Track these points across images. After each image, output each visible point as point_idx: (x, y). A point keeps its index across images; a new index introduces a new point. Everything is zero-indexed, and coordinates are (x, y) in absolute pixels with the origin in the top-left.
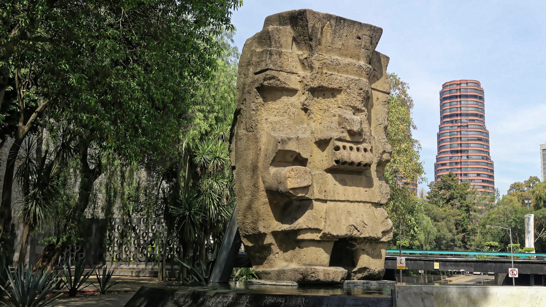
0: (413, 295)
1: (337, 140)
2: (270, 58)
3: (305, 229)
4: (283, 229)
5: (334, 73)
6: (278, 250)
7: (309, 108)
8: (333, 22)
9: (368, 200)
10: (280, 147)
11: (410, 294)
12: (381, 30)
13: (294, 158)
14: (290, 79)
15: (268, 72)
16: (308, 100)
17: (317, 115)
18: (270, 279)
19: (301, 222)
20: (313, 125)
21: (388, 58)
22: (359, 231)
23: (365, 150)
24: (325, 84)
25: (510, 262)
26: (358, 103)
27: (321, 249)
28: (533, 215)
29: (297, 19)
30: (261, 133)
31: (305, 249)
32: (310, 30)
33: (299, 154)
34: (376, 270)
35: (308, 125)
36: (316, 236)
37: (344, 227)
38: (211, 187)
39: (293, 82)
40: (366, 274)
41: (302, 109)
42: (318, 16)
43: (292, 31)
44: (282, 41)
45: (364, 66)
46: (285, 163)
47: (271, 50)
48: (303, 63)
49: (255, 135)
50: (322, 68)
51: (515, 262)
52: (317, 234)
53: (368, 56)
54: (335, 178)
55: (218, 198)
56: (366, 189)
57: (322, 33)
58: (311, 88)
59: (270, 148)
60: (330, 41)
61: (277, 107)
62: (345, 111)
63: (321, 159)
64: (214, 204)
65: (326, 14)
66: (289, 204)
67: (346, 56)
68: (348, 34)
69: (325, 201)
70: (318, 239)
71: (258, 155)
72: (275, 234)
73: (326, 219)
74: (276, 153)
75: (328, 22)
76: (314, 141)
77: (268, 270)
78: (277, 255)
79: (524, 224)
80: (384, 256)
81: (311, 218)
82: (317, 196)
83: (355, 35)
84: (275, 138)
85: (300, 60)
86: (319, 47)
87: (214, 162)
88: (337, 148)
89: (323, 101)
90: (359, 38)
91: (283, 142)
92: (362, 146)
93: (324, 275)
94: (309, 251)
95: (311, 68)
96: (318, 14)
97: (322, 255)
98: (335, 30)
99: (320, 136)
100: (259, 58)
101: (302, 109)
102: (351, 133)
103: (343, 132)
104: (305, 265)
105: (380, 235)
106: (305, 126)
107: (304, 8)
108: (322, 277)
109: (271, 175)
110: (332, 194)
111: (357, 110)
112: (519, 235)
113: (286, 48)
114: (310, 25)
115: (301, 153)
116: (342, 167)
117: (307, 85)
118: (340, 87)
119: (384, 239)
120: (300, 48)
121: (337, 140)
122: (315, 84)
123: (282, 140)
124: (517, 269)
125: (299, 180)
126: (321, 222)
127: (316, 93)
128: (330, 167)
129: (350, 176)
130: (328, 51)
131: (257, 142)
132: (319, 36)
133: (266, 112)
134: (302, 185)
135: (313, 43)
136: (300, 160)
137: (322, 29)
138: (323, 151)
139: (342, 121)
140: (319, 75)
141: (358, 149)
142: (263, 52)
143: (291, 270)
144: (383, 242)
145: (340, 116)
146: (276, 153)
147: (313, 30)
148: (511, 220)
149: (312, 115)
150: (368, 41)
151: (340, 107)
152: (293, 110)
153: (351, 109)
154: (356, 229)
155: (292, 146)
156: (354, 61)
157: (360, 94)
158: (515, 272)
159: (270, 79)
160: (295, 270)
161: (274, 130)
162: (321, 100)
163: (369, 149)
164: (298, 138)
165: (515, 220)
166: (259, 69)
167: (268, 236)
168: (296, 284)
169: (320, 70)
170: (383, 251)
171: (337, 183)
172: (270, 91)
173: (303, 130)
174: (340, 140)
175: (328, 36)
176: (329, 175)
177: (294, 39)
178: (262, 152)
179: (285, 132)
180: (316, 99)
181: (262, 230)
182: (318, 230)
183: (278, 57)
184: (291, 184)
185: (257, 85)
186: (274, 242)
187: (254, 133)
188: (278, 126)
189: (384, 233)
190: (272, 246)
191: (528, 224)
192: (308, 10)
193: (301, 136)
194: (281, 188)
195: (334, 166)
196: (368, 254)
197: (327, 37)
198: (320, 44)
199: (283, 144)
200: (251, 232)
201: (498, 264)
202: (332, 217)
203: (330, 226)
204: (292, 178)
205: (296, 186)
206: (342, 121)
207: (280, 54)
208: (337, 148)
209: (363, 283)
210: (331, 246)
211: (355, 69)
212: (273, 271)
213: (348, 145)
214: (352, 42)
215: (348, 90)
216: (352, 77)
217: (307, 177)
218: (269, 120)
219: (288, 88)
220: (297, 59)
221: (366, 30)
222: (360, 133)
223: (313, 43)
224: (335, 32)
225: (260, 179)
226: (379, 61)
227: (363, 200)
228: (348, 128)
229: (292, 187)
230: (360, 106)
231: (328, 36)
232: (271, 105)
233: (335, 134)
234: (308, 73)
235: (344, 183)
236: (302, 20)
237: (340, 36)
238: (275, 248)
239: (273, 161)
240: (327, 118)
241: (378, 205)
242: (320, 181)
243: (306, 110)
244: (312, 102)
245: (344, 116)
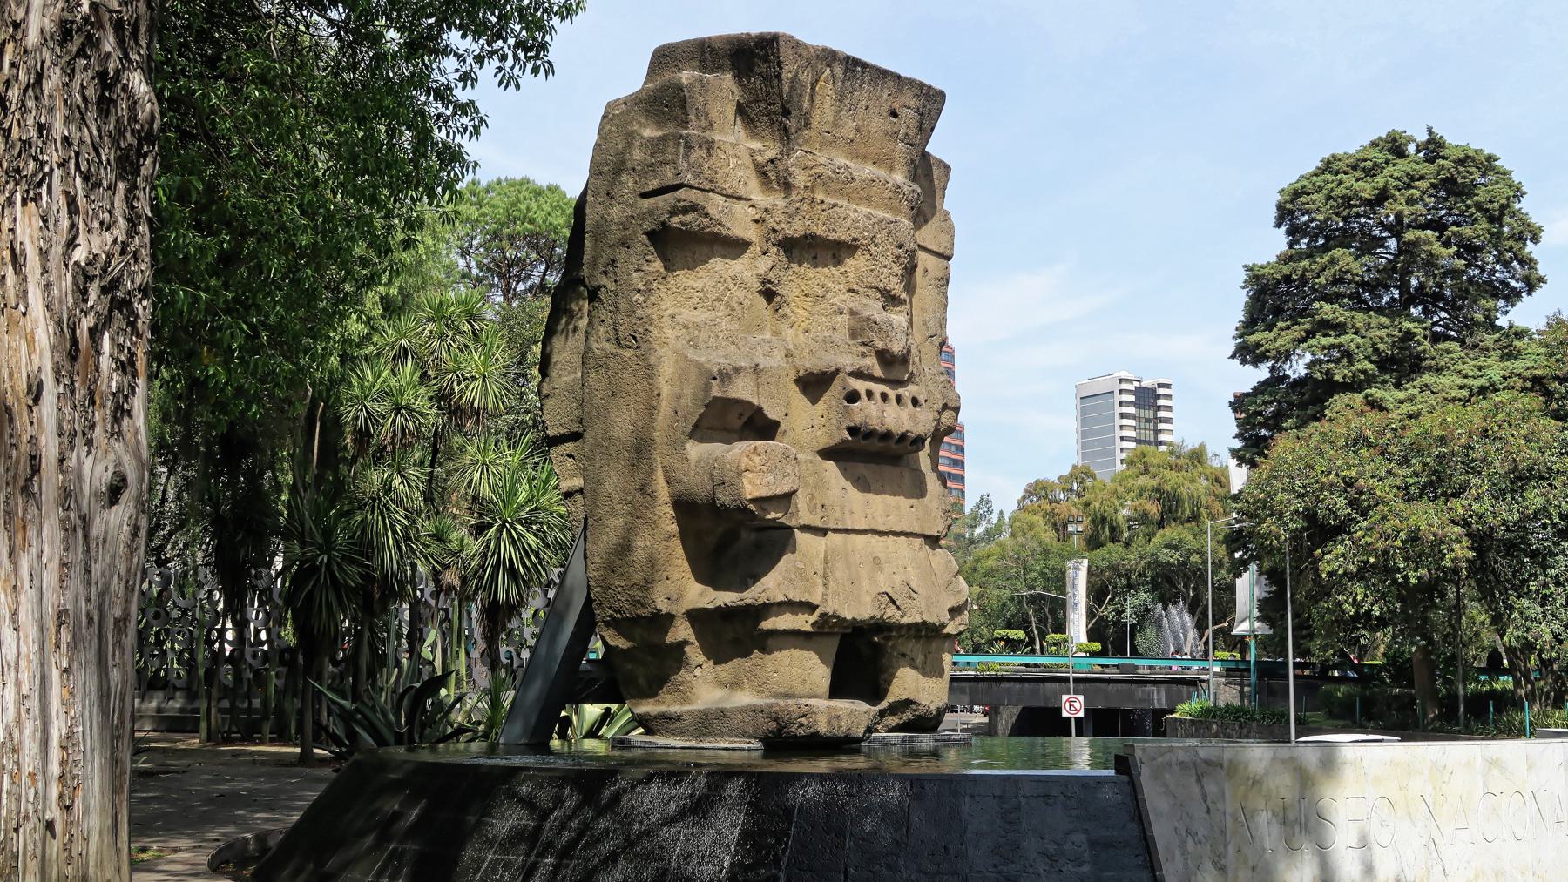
0: (1177, 768)
1: (852, 374)
2: (686, 156)
3: (781, 604)
4: (720, 603)
6: (701, 658)
7: (779, 290)
8: (838, 70)
9: (917, 530)
10: (716, 392)
11: (1169, 764)
12: (941, 95)
13: (744, 419)
14: (731, 213)
15: (681, 193)
16: (776, 271)
17: (798, 309)
18: (679, 733)
19: (772, 585)
20: (789, 333)
21: (947, 168)
22: (898, 608)
23: (915, 402)
24: (820, 231)
25: (1066, 680)
26: (894, 280)
27: (812, 655)
28: (1086, 562)
29: (752, 58)
30: (661, 351)
31: (776, 654)
32: (786, 88)
33: (760, 409)
34: (933, 707)
35: (776, 333)
36: (804, 622)
37: (868, 599)
38: (387, 488)
39: (739, 222)
40: (908, 715)
41: (760, 292)
42: (805, 53)
43: (735, 88)
44: (713, 114)
45: (906, 189)
46: (730, 435)
47: (688, 136)
48: (764, 174)
49: (644, 358)
50: (813, 191)
51: (1076, 680)
52: (806, 616)
54: (844, 472)
55: (406, 517)
56: (912, 501)
58: (786, 238)
59: (688, 391)
60: (831, 119)
61: (699, 284)
62: (865, 300)
63: (809, 424)
64: (394, 532)
65: (824, 49)
66: (735, 538)
68: (871, 103)
69: (822, 532)
70: (808, 628)
71: (651, 409)
72: (697, 617)
73: (825, 577)
74: (707, 406)
76: (793, 376)
77: (675, 709)
78: (698, 672)
79: (1064, 585)
80: (948, 671)
82: (805, 517)
83: (886, 107)
84: (699, 366)
85: (756, 165)
87: (394, 421)
88: (853, 397)
89: (811, 273)
90: (895, 115)
91: (725, 376)
92: (907, 392)
93: (829, 721)
94: (786, 662)
95: (787, 187)
96: (807, 47)
97: (806, 672)
99: (808, 365)
100: (652, 155)
101: (760, 292)
102: (885, 357)
103: (863, 355)
104: (776, 695)
105: (945, 617)
106: (768, 336)
107: (773, 30)
108: (823, 728)
109: (693, 462)
110: (838, 515)
111: (891, 300)
112: (1053, 611)
113: (721, 131)
114: (786, 75)
115: (765, 408)
117: (774, 230)
118: (855, 240)
119: (951, 629)
120: (753, 133)
121: (852, 374)
122: (796, 229)
123: (720, 371)
124: (1081, 698)
125: (771, 478)
126: (814, 585)
127: (796, 252)
128: (832, 443)
130: (825, 144)
131: (650, 376)
132: (806, 105)
133: (672, 298)
134: (779, 491)
135: (792, 123)
136: (759, 426)
137: (813, 88)
138: (814, 401)
139: (860, 328)
140: (805, 207)
141: (899, 399)
142: (664, 138)
143: (743, 710)
144: (948, 636)
145: (853, 313)
146: (707, 406)
147: (791, 88)
148: (1034, 575)
149: (785, 310)
150: (914, 123)
152: (739, 293)
154: (894, 602)
155: (742, 389)
156: (882, 173)
157: (898, 257)
158: (1077, 705)
159: (685, 211)
160: (755, 710)
161: (695, 346)
162: (806, 270)
163: (921, 398)
164: (756, 369)
165: (1042, 574)
166: (654, 184)
167: (678, 622)
168: (758, 745)
169: (807, 194)
170: (947, 659)
171: (848, 485)
172: (682, 243)
173: (766, 347)
174: (859, 374)
175: (827, 104)
176: (830, 464)
177: (741, 110)
178: (664, 403)
179: (721, 352)
180: (795, 267)
181: (663, 606)
182: (811, 608)
183: (703, 153)
184: (753, 487)
185: (647, 226)
186: (692, 638)
187: (639, 352)
188: (703, 335)
189: (955, 611)
190: (687, 648)
191: (1074, 586)
192: (784, 35)
193: (763, 363)
194: (724, 497)
195: (845, 441)
196: (915, 668)
197: (824, 108)
198: (807, 125)
199: (722, 381)
200: (630, 611)
201: (1026, 685)
202: (840, 572)
203: (836, 594)
204: (752, 471)
205: (765, 492)
206: (860, 328)
207: (709, 146)
208: (853, 397)
209: (903, 741)
210: (833, 645)
211: (888, 194)
212: (690, 712)
213: (878, 388)
214: (879, 123)
215: (873, 248)
216: (880, 214)
217: (789, 469)
218: (678, 318)
220: (748, 161)
221: (910, 94)
222: (904, 360)
223: (792, 123)
224: (841, 97)
225: (660, 473)
226: (929, 175)
228: (880, 345)
229: (756, 494)
230: (897, 289)
231: (827, 104)
232: (684, 279)
233: (848, 361)
234: (777, 200)
235: (863, 485)
236: (766, 60)
237: (853, 108)
238: (695, 654)
239: (696, 426)
240: (820, 317)
241: (933, 541)
242: (811, 480)
243: (769, 295)
244: (789, 275)
245: (867, 314)
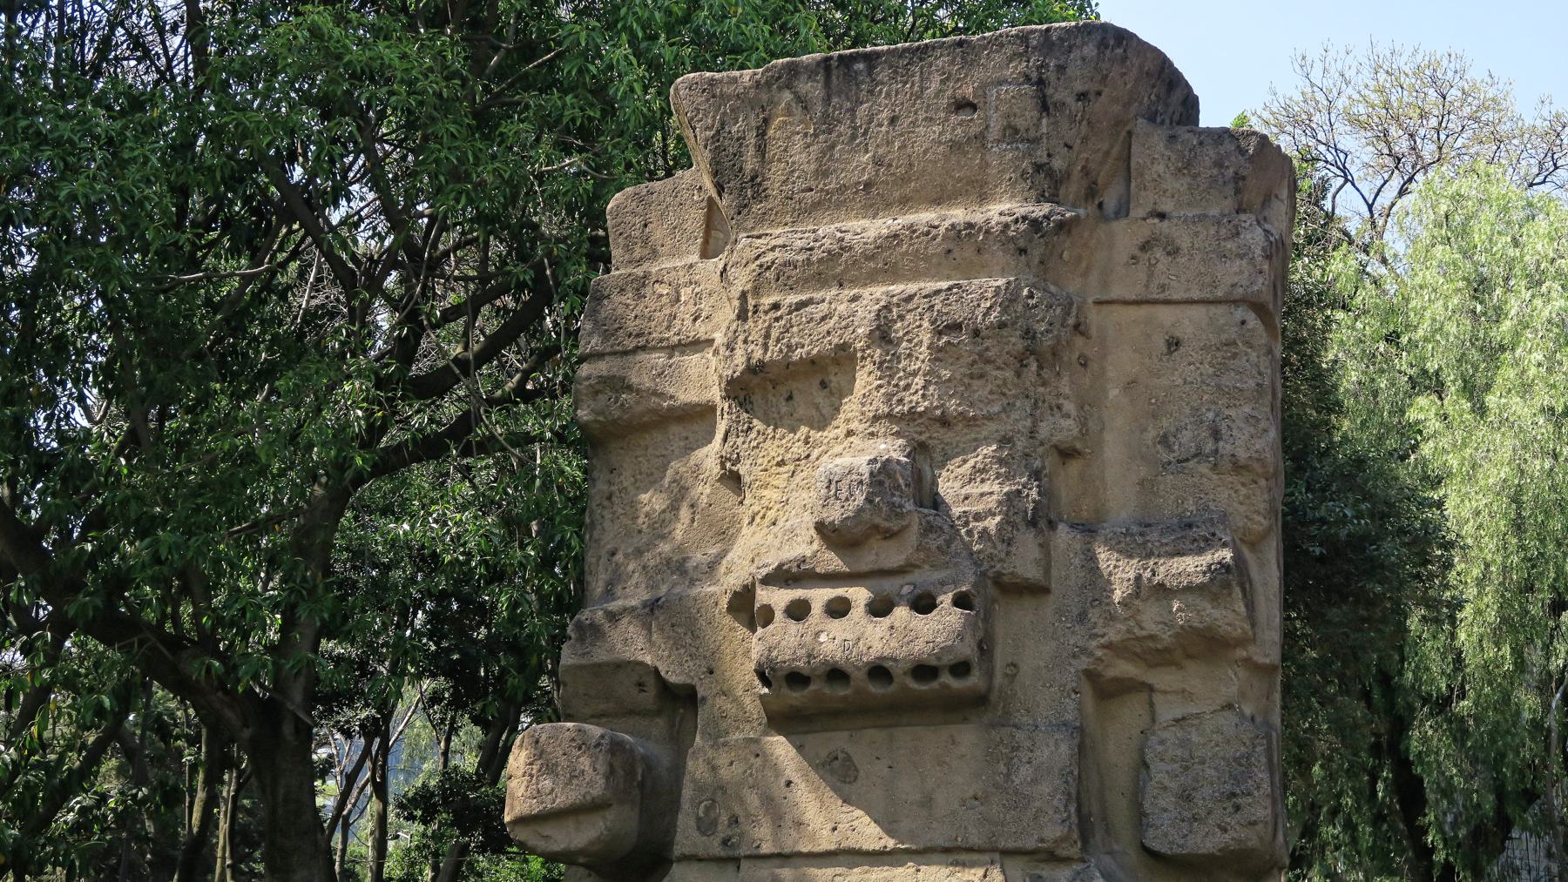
1: (767, 581)
5: (817, 296)
9: (975, 839)
16: (731, 441)
33: (656, 671)
53: (1038, 168)
57: (761, 150)
67: (905, 203)
75: (787, 96)
86: (757, 208)
98: (825, 115)
116: (795, 697)
121: (767, 581)
129: (877, 735)
132: (750, 163)
137: (762, 134)
198: (760, 194)
199: (581, 639)
208: (767, 615)
211: (936, 248)
213: (819, 596)
216: (912, 288)
219: (670, 408)
227: (941, 841)
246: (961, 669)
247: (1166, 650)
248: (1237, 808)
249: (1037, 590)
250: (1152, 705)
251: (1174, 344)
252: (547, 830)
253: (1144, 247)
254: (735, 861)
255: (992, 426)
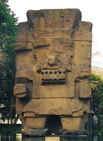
33: (28, 79)
81: (29, 107)
93: (32, 133)
115: (29, 78)
134: (20, 93)
151: (50, 53)
153: (55, 53)
213: (49, 71)
227: (62, 97)
246: (64, 79)
247: (82, 78)
248: (88, 93)
249: (70, 71)
250: (80, 83)
251: (83, 45)
252: (19, 95)
253: (80, 35)
254: (39, 98)
255: (65, 54)
